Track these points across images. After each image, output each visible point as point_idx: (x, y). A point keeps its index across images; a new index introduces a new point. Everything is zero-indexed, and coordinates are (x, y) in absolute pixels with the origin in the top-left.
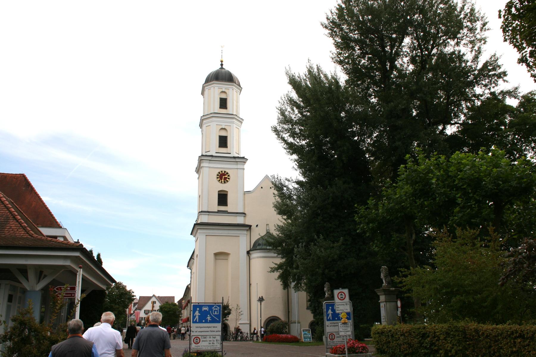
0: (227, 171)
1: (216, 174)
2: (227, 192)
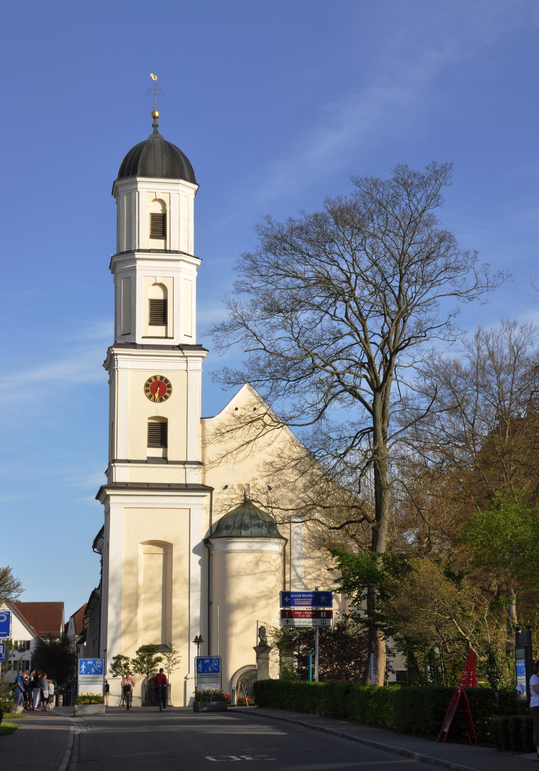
2: (167, 419)
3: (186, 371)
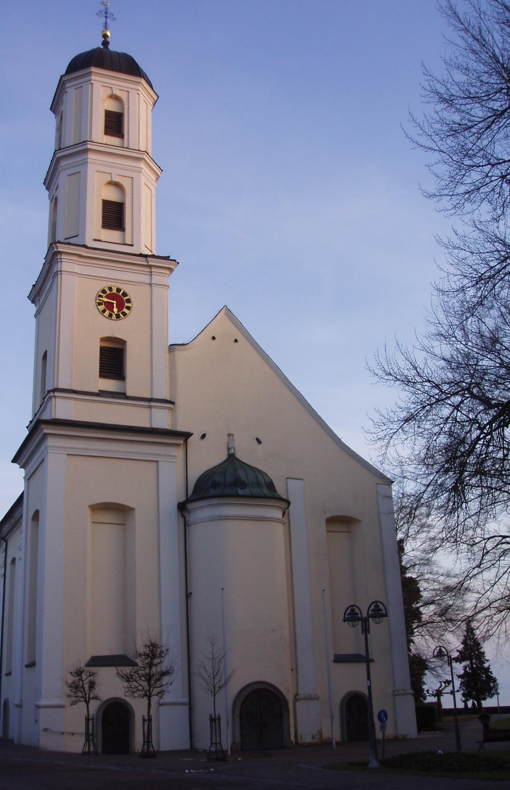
0: (125, 288)
1: (94, 295)
2: (123, 342)
3: (150, 284)
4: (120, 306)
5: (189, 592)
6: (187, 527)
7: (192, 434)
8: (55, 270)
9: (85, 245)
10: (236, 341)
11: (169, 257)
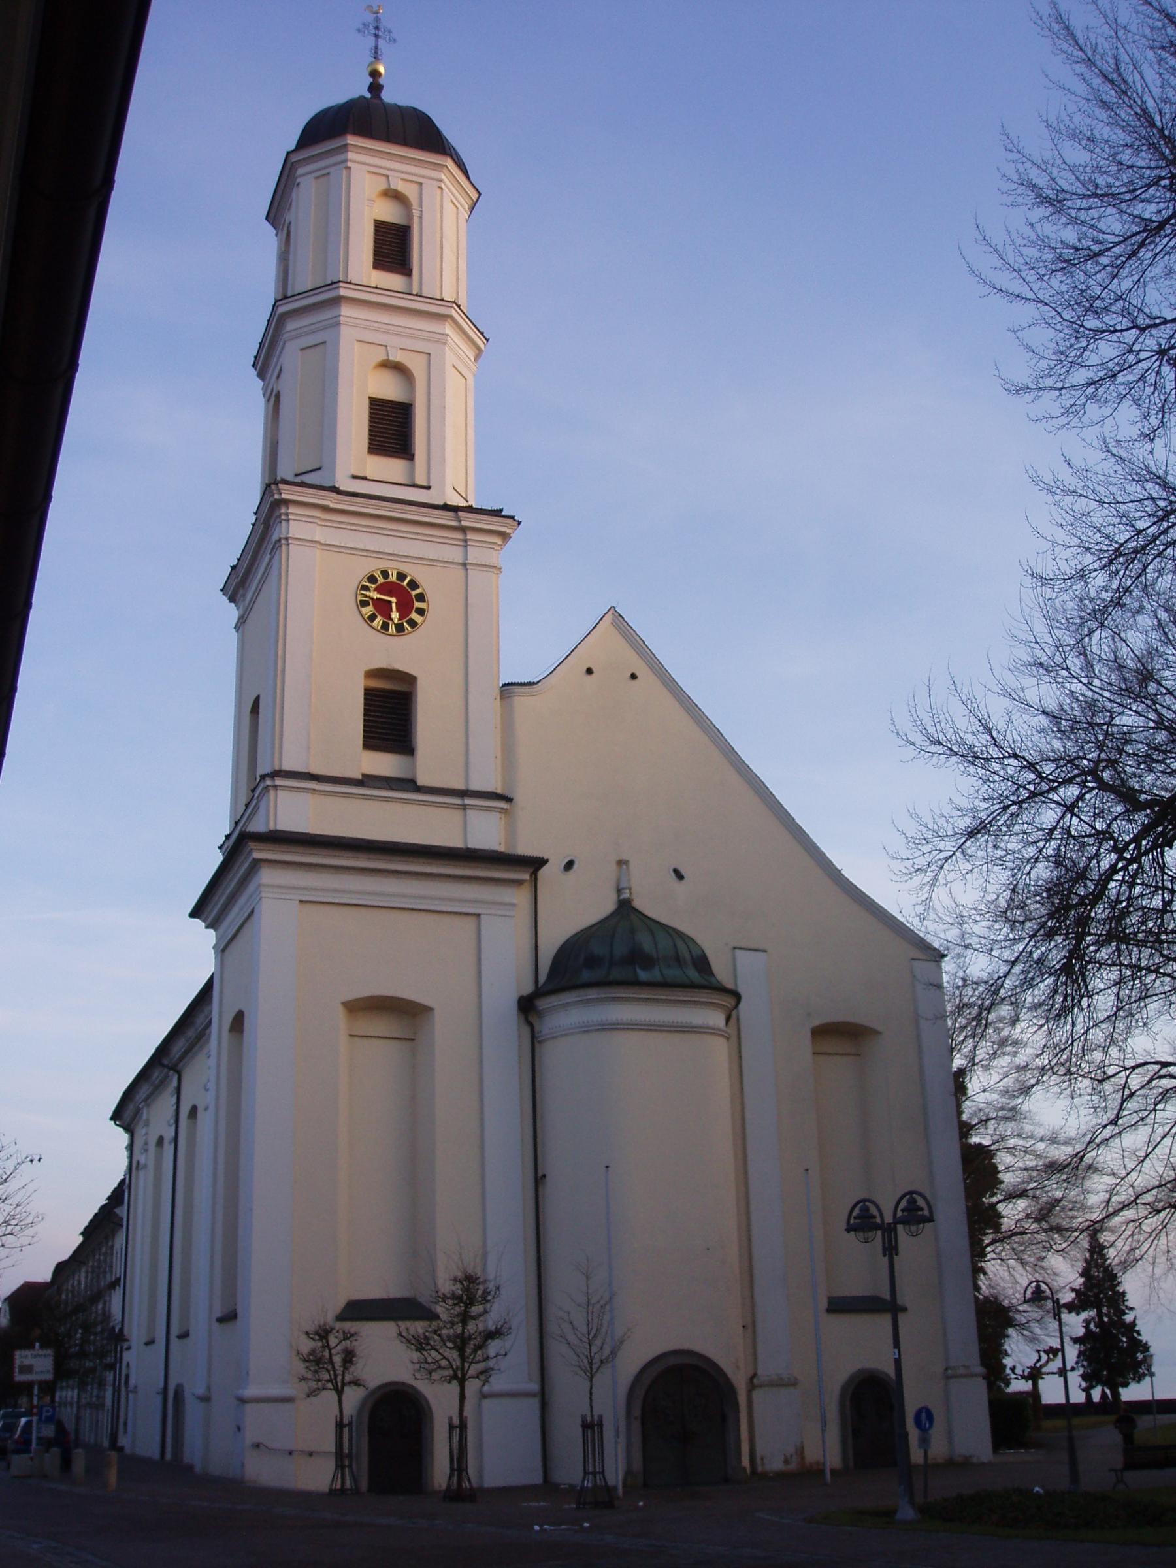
1: (354, 585)
2: (410, 680)
3: (464, 565)
4: (405, 607)
5: (540, 1174)
6: (537, 1045)
7: (547, 861)
8: (275, 537)
9: (334, 487)
10: (633, 677)
11: (501, 510)
